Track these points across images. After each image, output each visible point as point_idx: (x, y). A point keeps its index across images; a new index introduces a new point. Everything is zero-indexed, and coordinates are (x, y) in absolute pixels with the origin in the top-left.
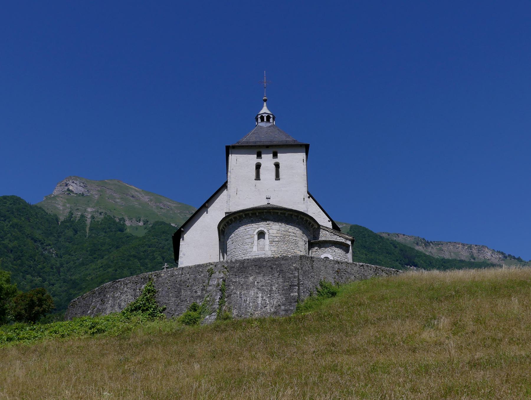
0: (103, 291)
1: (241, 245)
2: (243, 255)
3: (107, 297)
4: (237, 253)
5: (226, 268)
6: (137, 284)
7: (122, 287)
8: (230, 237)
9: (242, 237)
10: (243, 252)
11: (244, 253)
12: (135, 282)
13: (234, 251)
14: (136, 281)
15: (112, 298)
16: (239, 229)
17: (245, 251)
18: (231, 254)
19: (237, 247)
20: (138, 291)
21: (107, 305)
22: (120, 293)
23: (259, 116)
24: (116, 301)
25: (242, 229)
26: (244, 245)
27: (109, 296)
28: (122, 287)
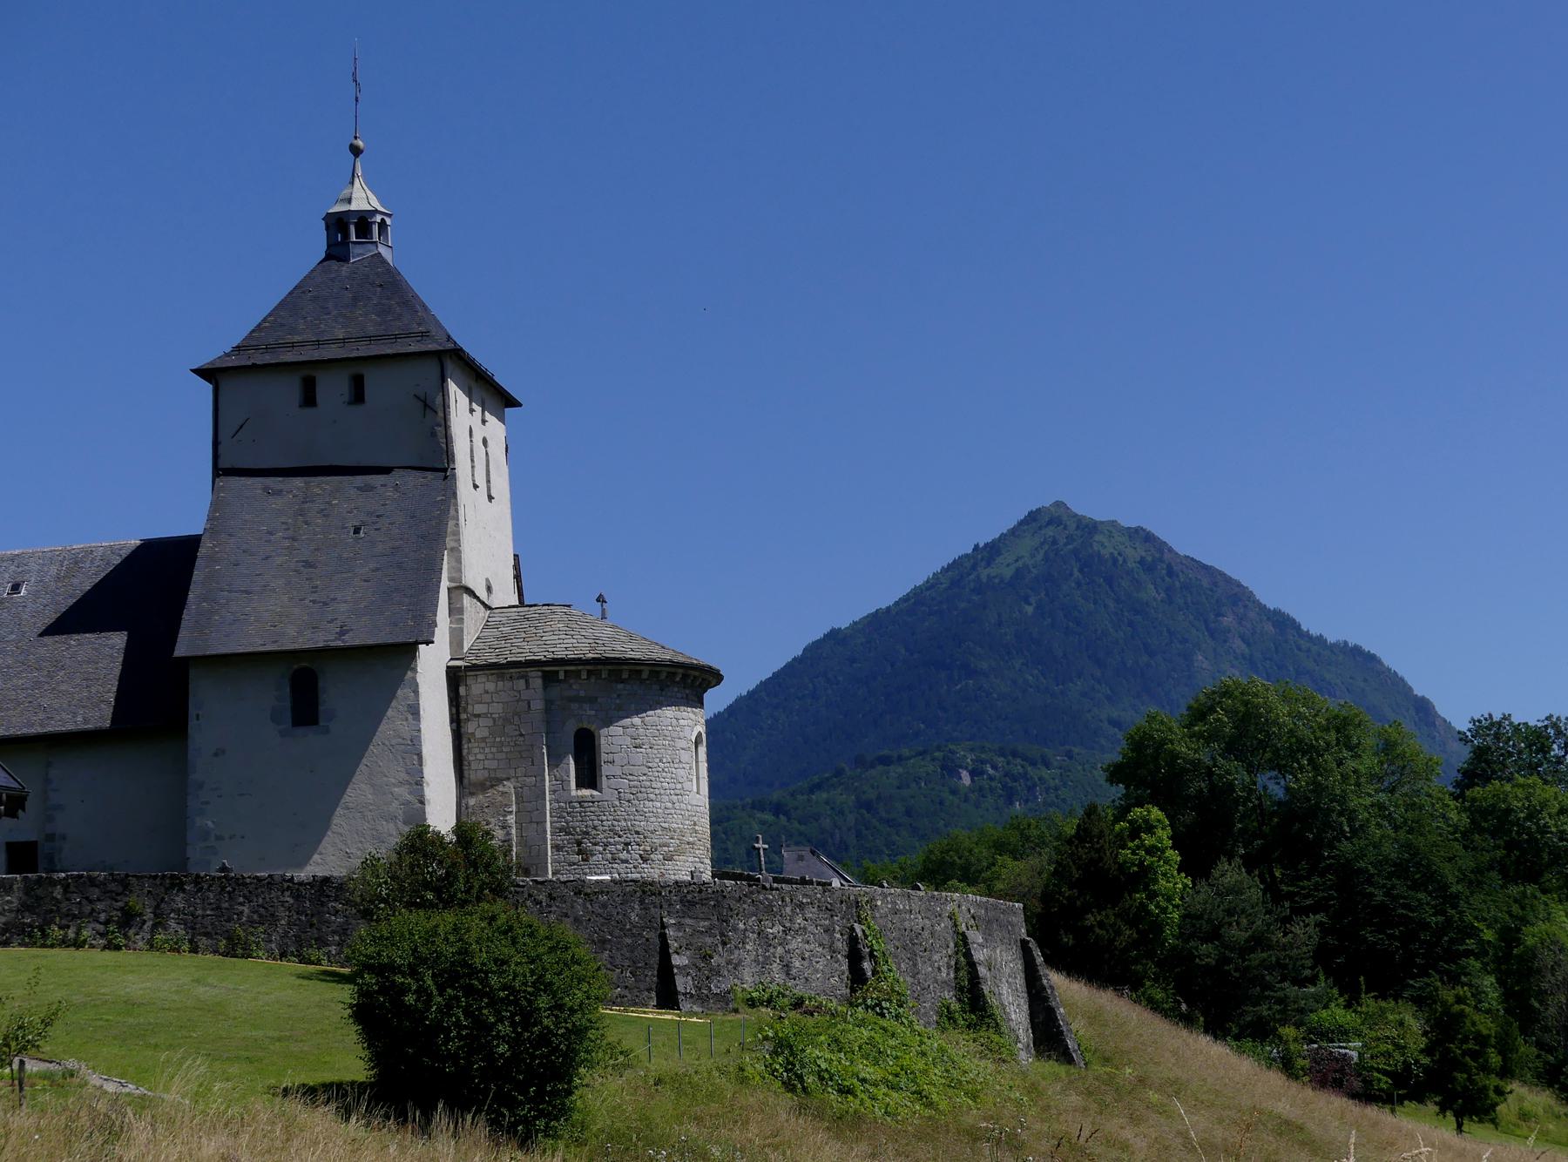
0: (712, 903)
1: (668, 765)
2: (676, 797)
3: (735, 929)
4: (659, 785)
5: (973, 917)
6: (832, 916)
7: (788, 910)
8: (627, 721)
9: (669, 738)
10: (673, 786)
11: (678, 792)
12: (827, 908)
13: (644, 775)
14: (829, 906)
15: (755, 935)
16: (659, 711)
17: (679, 786)
18: (631, 777)
19: (656, 765)
20: (838, 936)
21: (737, 952)
22: (784, 926)
23: (378, 218)
24: (772, 950)
25: (669, 713)
26: (676, 766)
27: (741, 926)
28: (788, 910)
